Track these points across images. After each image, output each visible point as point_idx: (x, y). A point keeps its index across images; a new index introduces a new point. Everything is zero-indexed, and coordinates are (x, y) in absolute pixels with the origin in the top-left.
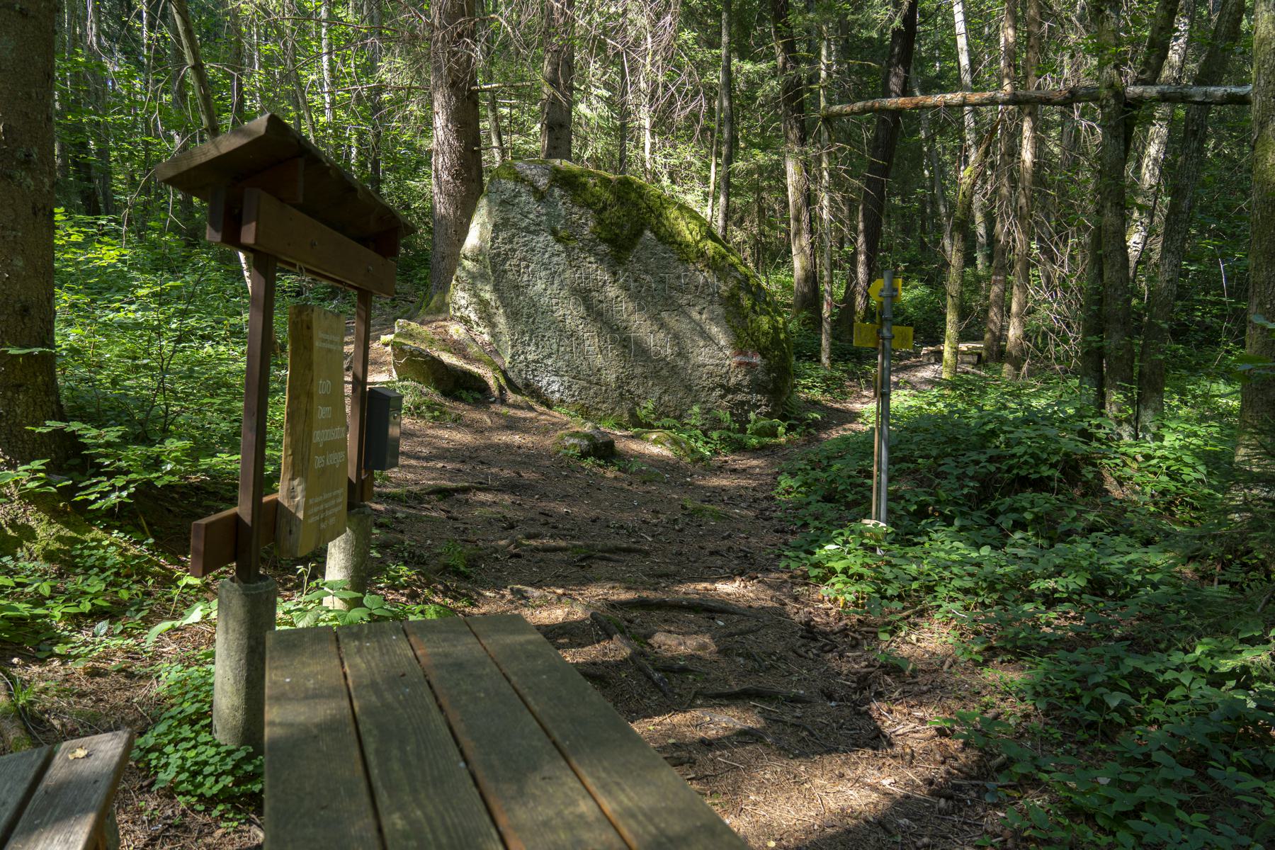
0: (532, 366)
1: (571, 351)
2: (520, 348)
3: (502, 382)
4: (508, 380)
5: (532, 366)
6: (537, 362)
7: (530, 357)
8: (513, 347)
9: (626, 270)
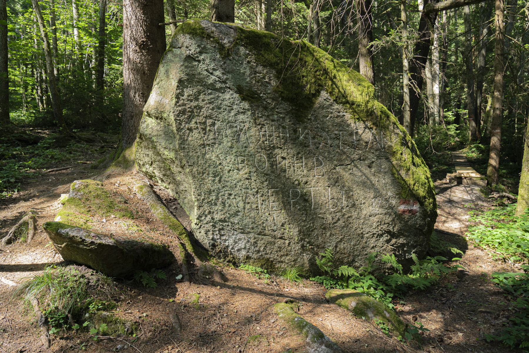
0: (218, 226)
1: (257, 208)
2: (206, 208)
3: (189, 248)
4: (195, 243)
5: (218, 226)
6: (224, 221)
7: (217, 217)
8: (199, 207)
9: (305, 128)
